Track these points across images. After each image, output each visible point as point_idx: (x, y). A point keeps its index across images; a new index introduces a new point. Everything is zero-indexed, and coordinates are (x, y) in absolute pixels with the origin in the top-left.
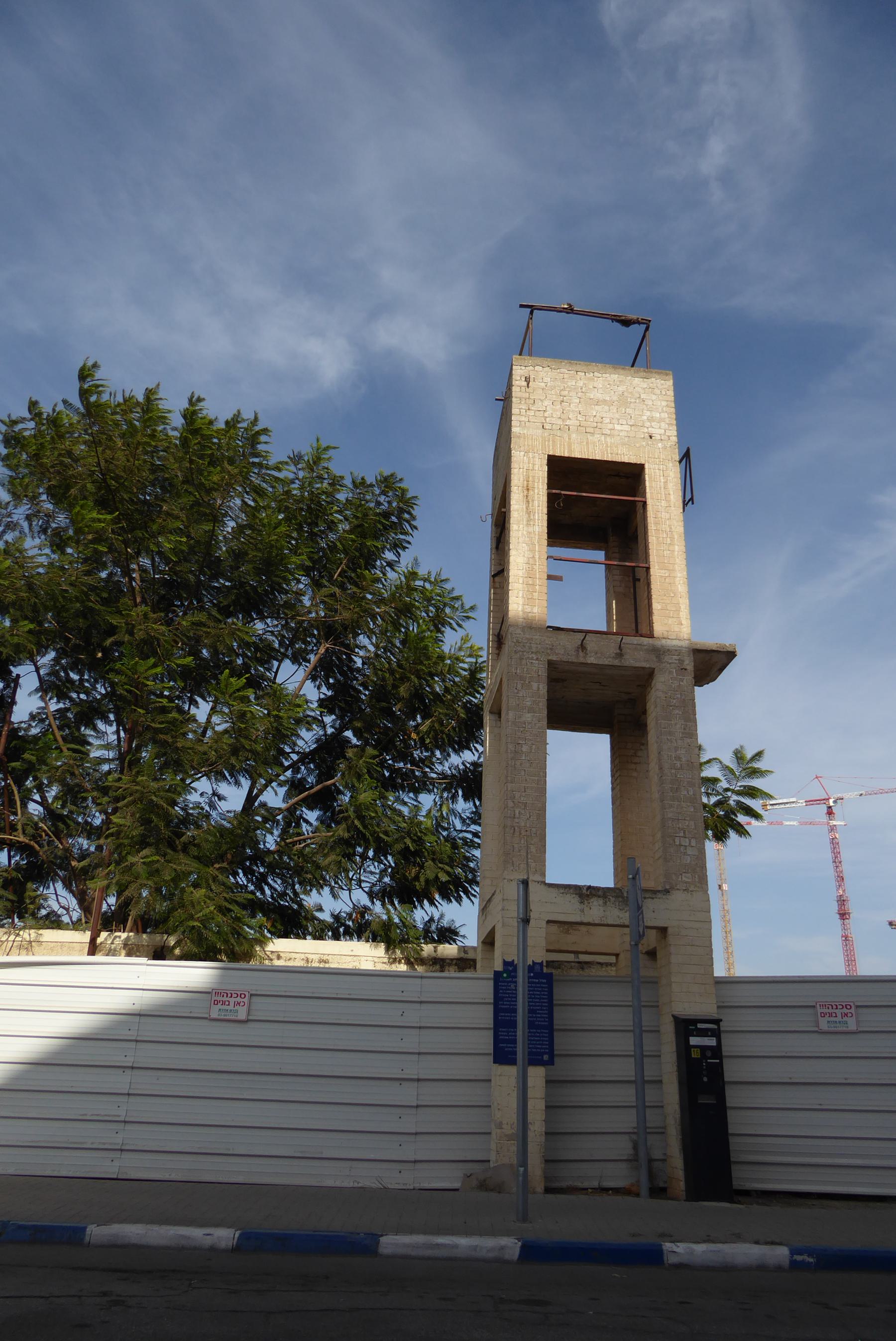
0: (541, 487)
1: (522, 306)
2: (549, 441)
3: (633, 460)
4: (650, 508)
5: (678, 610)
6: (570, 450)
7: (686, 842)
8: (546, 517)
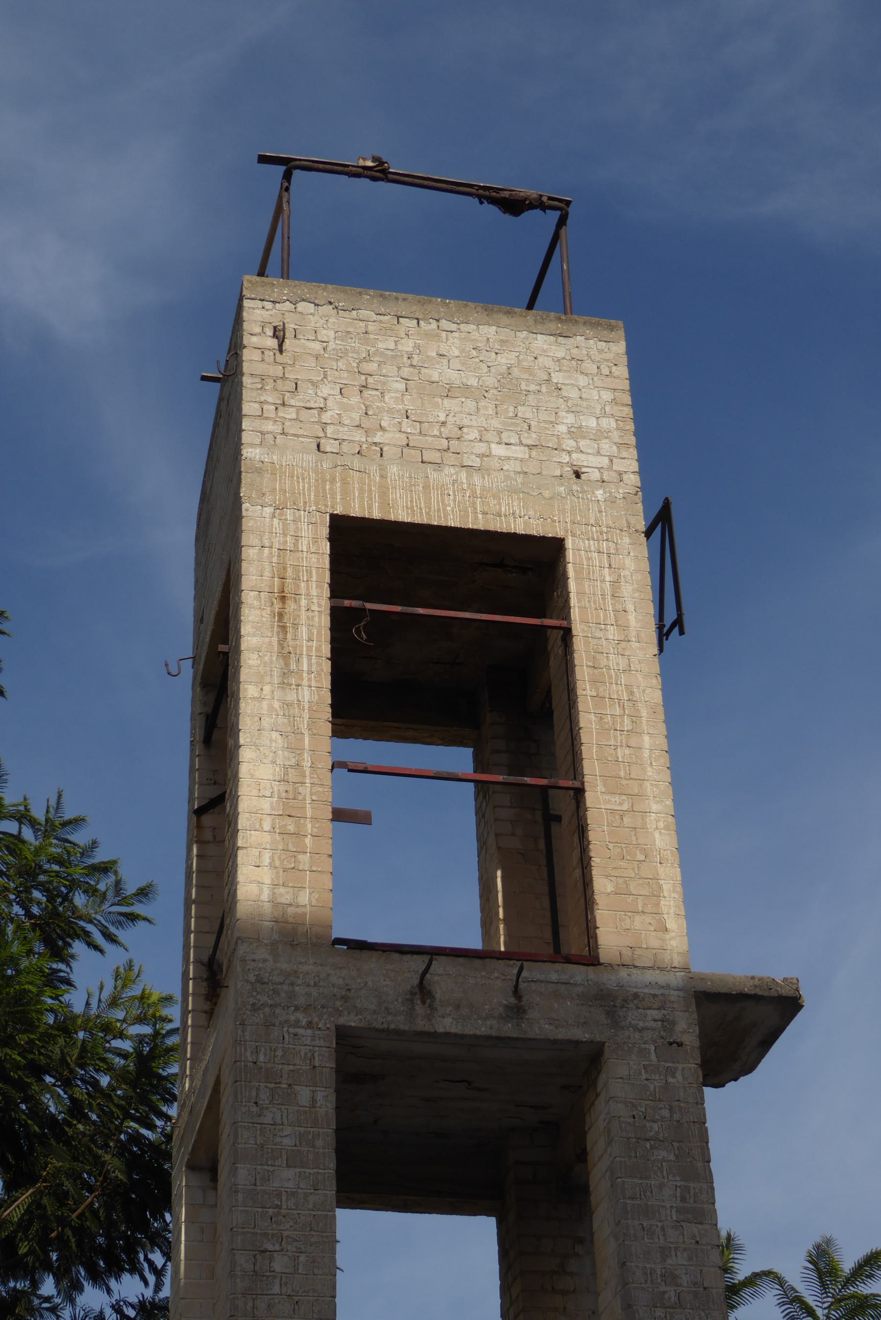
0: (314, 592)
1: (263, 159)
2: (333, 481)
3: (536, 528)
4: (579, 644)
5: (656, 895)
6: (385, 504)
8: (327, 666)
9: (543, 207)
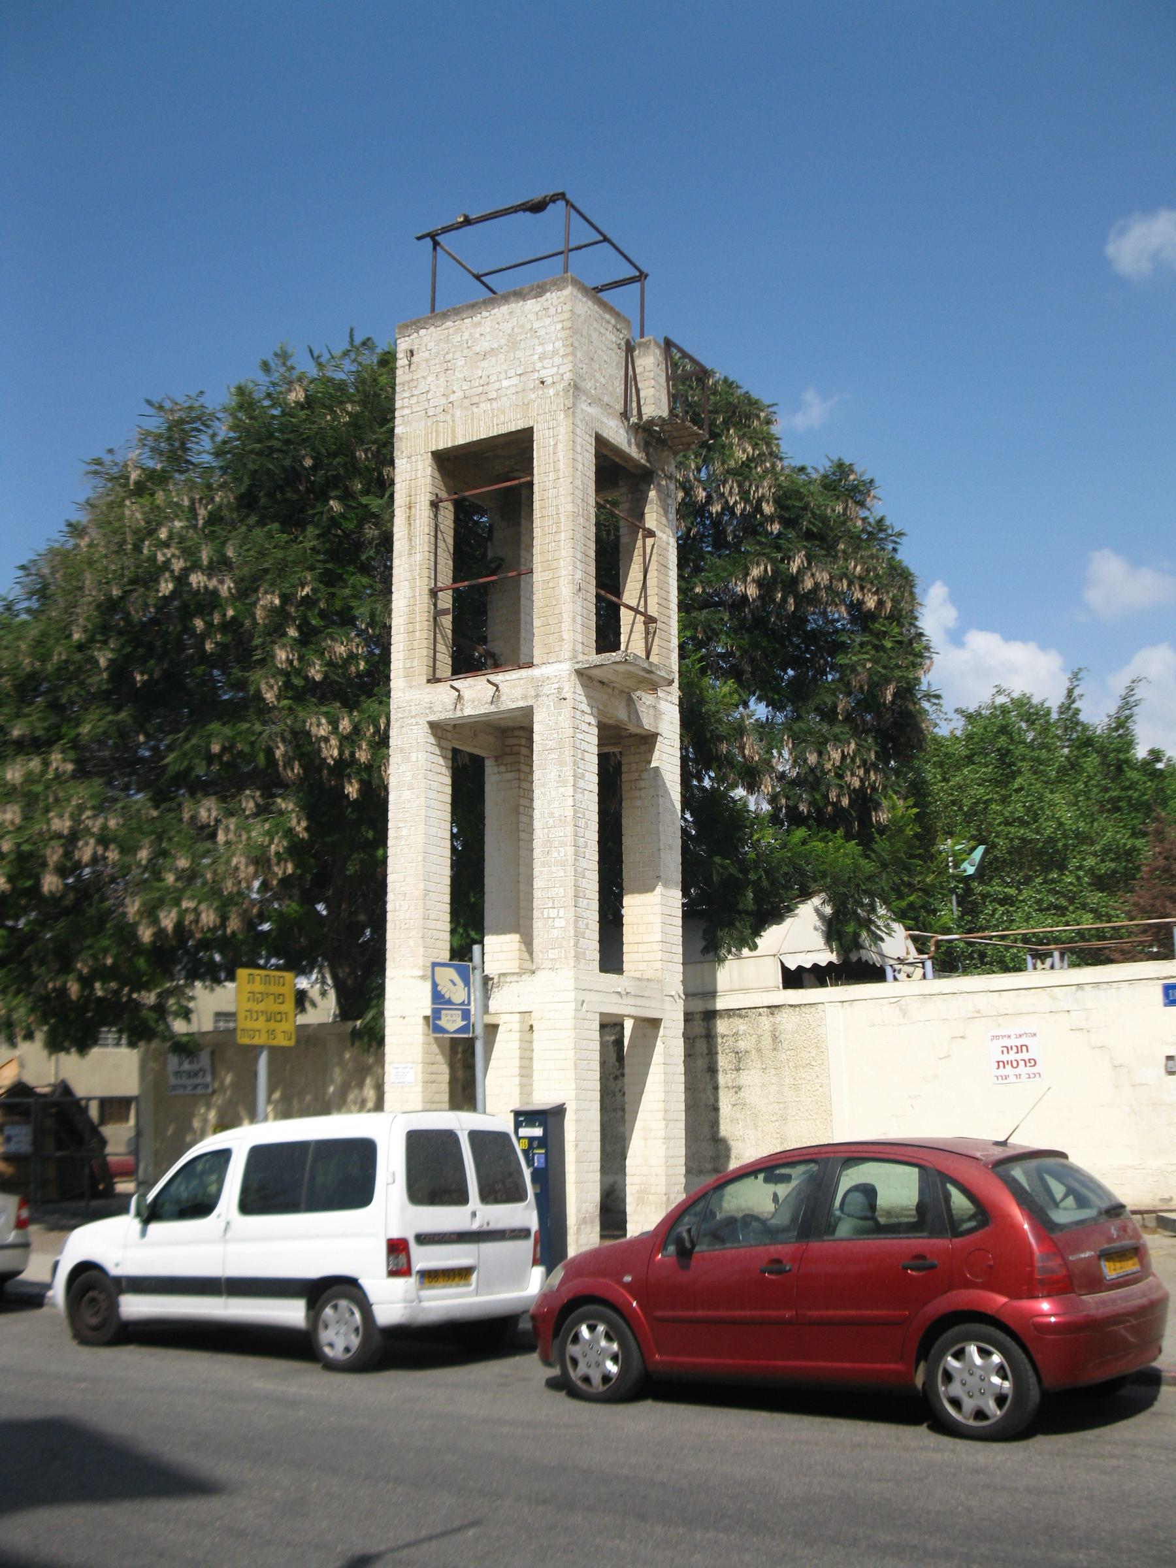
1: (419, 238)
4: (536, 488)
7: (553, 913)
9: (554, 201)
